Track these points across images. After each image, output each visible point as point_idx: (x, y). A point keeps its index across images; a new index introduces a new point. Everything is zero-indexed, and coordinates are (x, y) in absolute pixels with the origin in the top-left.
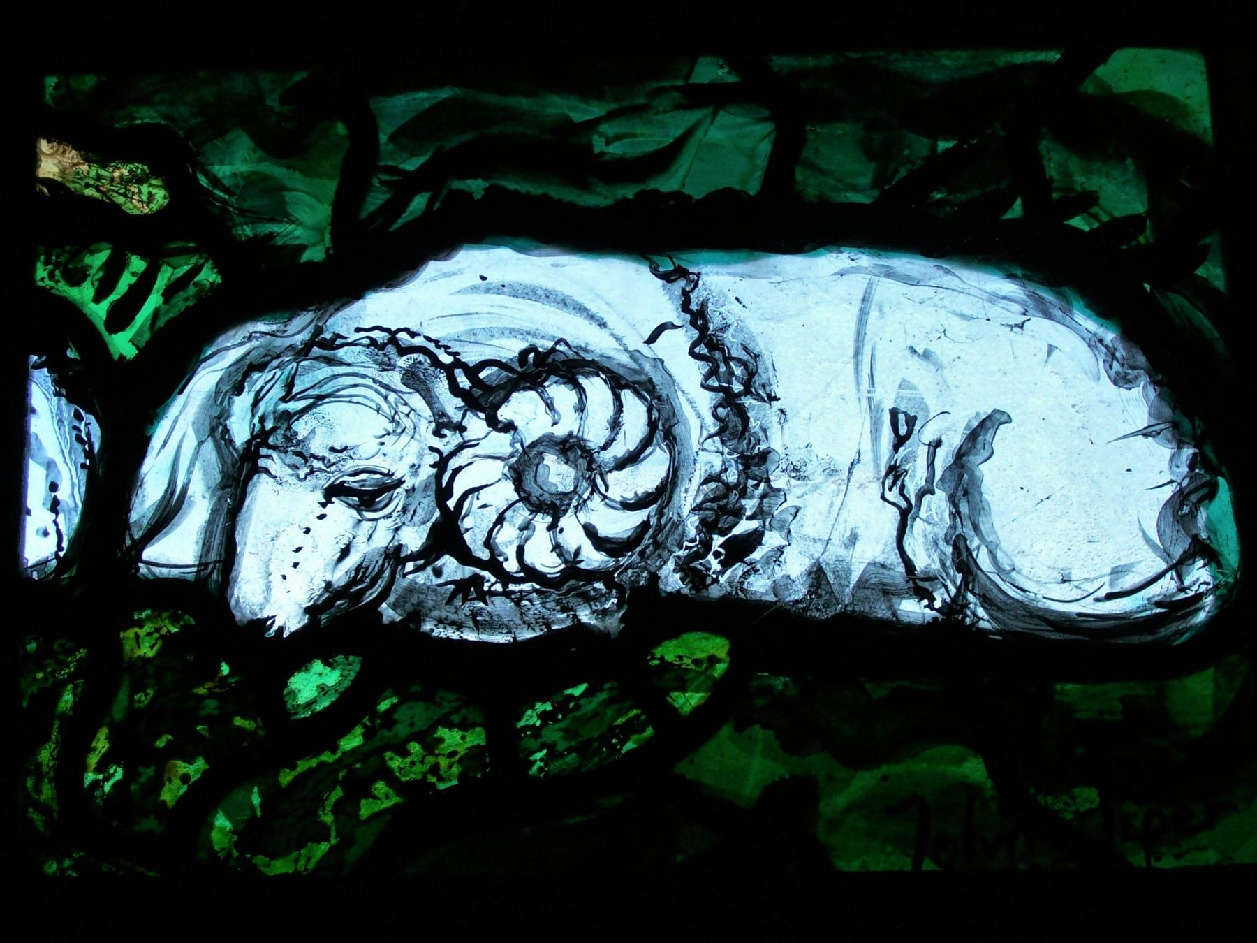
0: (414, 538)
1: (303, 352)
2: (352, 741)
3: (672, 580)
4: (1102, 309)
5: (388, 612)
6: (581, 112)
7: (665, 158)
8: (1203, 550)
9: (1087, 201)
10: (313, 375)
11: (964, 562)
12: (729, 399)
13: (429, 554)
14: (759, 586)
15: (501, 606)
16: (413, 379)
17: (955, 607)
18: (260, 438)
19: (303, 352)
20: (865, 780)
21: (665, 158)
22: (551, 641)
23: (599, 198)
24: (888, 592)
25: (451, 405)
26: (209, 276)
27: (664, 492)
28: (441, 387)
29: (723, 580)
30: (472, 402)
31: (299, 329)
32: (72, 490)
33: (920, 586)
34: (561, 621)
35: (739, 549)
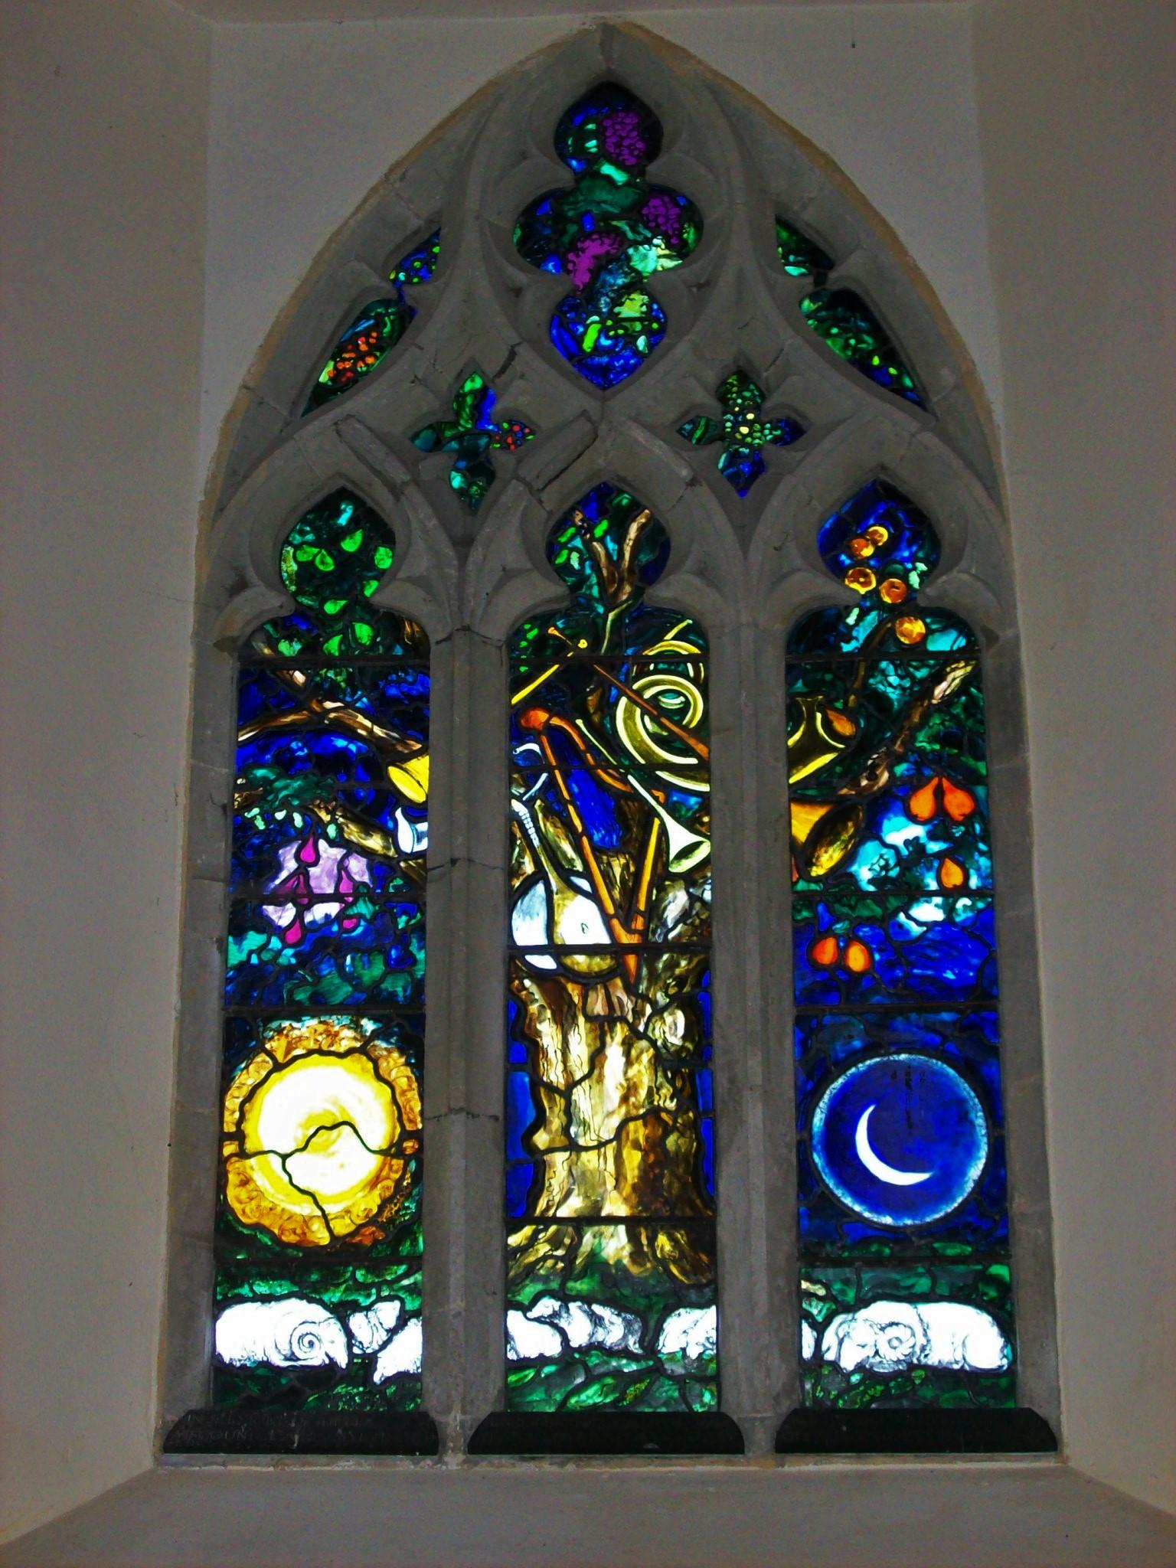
0: (872, 1354)
1: (851, 1321)
2: (862, 1388)
3: (915, 1361)
4: (989, 1313)
5: (867, 1366)
6: (897, 1277)
7: (912, 1286)
8: (1005, 1356)
9: (985, 1294)
10: (853, 1324)
11: (964, 1359)
12: (925, 1330)
13: (874, 1356)
14: (930, 1362)
15: (887, 1366)
16: (871, 1326)
17: (963, 1366)
18: (845, 1336)
19: (851, 1321)
20: (947, 1396)
21: (912, 1286)
22: (895, 1371)
23: (903, 1293)
24: (951, 1363)
25: (878, 1331)
26: (834, 1307)
27: (913, 1347)
28: (875, 1326)
29: (923, 1360)
30: (880, 1329)
31: (850, 1316)
32: (812, 1343)
33: (957, 1362)
34: (896, 1368)
35: (926, 1356)
